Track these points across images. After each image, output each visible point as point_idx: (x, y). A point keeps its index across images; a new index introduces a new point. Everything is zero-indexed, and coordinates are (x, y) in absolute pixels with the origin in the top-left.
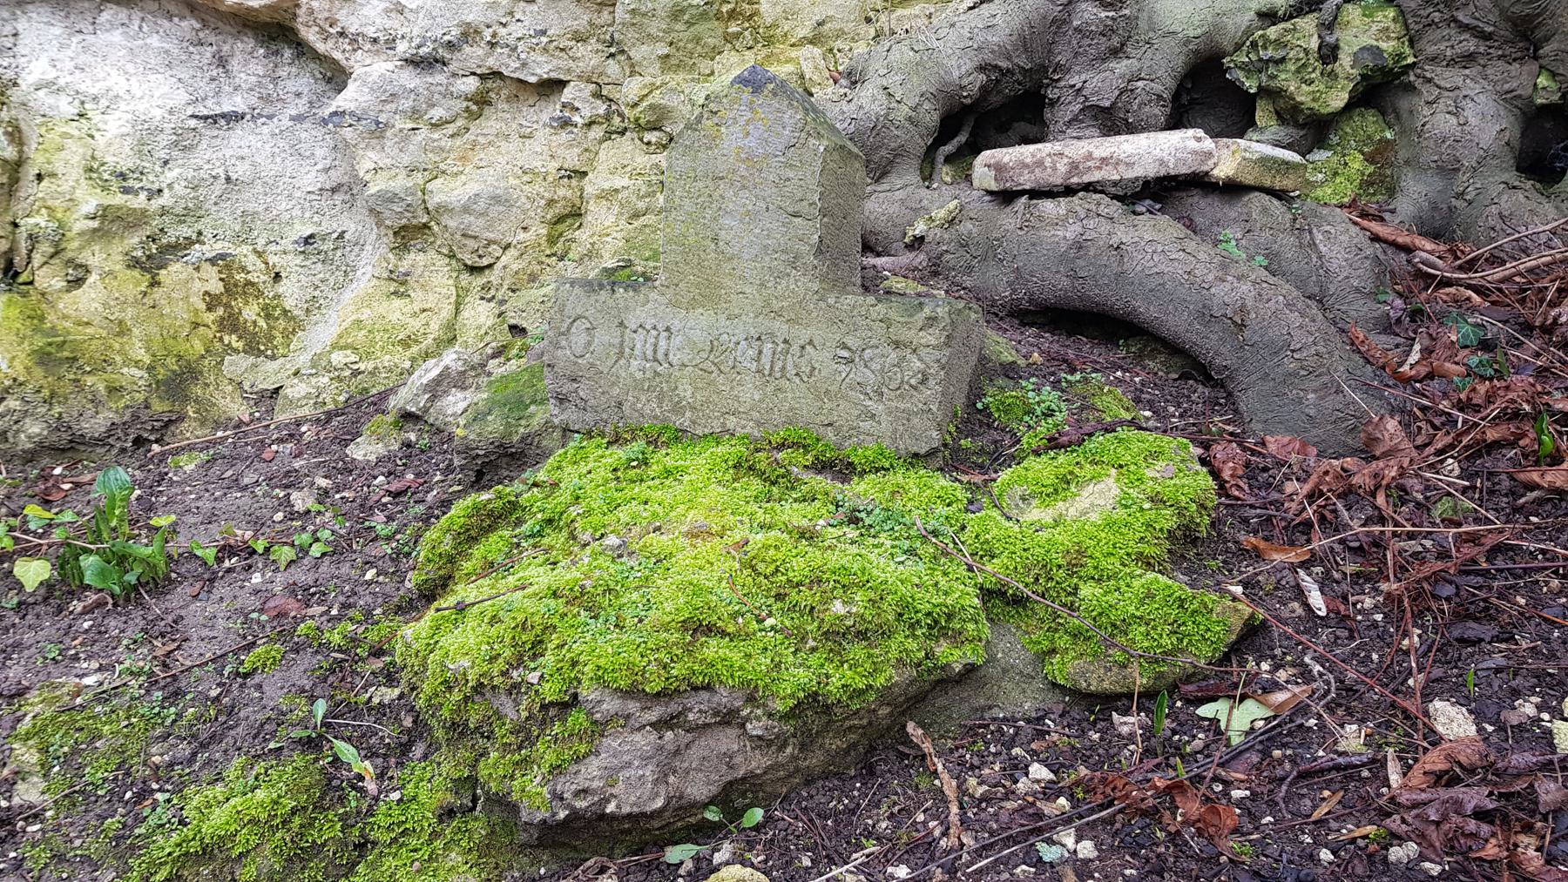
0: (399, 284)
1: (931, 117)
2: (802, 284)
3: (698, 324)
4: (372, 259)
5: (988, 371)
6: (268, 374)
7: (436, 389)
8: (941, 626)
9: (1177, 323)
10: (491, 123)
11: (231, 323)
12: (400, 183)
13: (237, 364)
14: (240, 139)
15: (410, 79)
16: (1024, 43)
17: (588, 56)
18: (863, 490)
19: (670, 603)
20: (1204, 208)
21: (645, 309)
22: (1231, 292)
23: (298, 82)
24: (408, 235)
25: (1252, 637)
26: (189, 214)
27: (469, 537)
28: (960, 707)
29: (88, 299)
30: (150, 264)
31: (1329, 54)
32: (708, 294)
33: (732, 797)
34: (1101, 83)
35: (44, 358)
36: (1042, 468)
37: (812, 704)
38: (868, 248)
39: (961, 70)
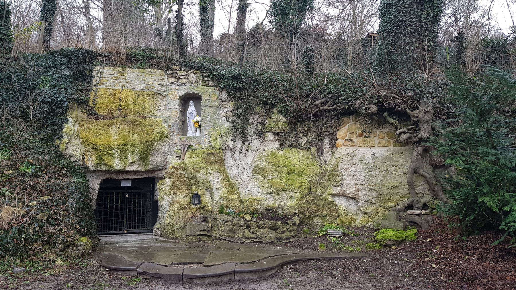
0: (364, 217)
1: (404, 208)
2: (396, 221)
3: (390, 222)
4: (361, 215)
5: (406, 225)
6: (355, 224)
7: (370, 225)
8: (403, 237)
9: (418, 223)
10: (371, 206)
11: (352, 220)
12: (364, 210)
13: (353, 223)
14: (351, 206)
15: (365, 203)
16: (411, 202)
17: (378, 201)
18: (399, 231)
19: (389, 235)
20: (422, 216)
21: (386, 222)
22: (421, 221)
23: (355, 202)
24: (365, 214)
25: (418, 238)
26: (349, 212)
27: (377, 234)
28: (404, 241)
29: (344, 218)
30: (347, 216)
31: (433, 204)
32: (390, 221)
33: (393, 244)
34: (417, 205)
35: (341, 222)
36: (409, 231)
37: (396, 240)
38: (400, 217)
39: (406, 205)
